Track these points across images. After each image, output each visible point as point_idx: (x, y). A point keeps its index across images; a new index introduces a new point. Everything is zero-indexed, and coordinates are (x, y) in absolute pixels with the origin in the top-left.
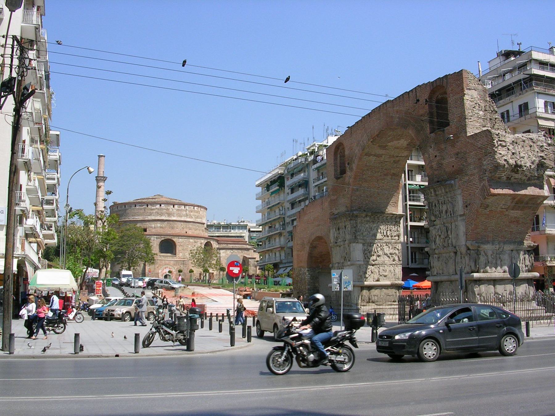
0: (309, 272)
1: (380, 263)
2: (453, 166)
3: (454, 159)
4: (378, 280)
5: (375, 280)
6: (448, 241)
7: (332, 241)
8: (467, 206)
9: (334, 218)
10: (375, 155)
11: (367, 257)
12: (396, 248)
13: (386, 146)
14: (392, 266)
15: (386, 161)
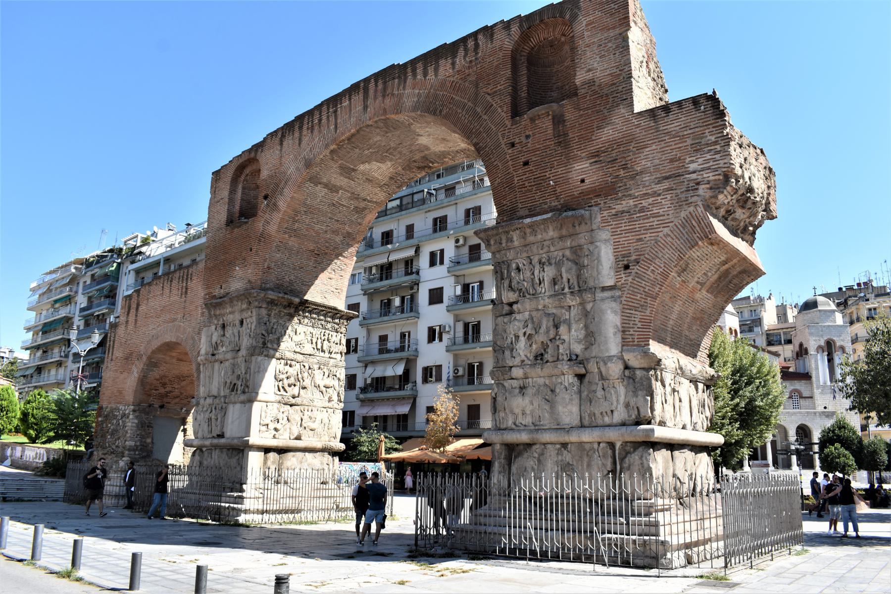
0: (137, 414)
1: (305, 402)
2: (583, 181)
3: (587, 165)
4: (298, 438)
5: (292, 438)
6: (558, 349)
7: (203, 352)
8: (627, 267)
9: (214, 303)
10: (326, 186)
11: (283, 387)
12: (336, 376)
13: (354, 170)
14: (325, 410)
15: (343, 205)
